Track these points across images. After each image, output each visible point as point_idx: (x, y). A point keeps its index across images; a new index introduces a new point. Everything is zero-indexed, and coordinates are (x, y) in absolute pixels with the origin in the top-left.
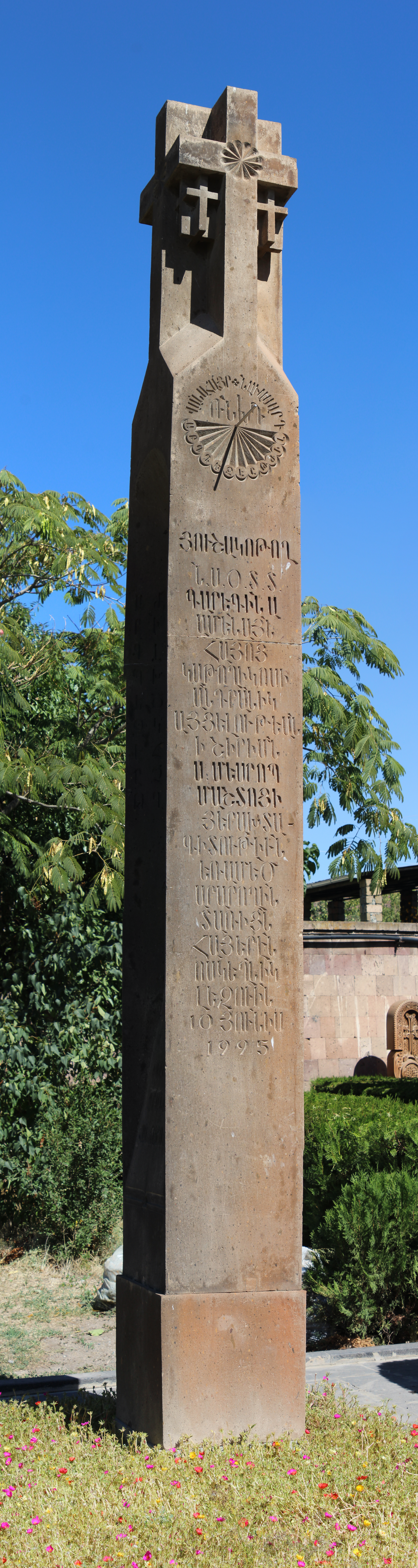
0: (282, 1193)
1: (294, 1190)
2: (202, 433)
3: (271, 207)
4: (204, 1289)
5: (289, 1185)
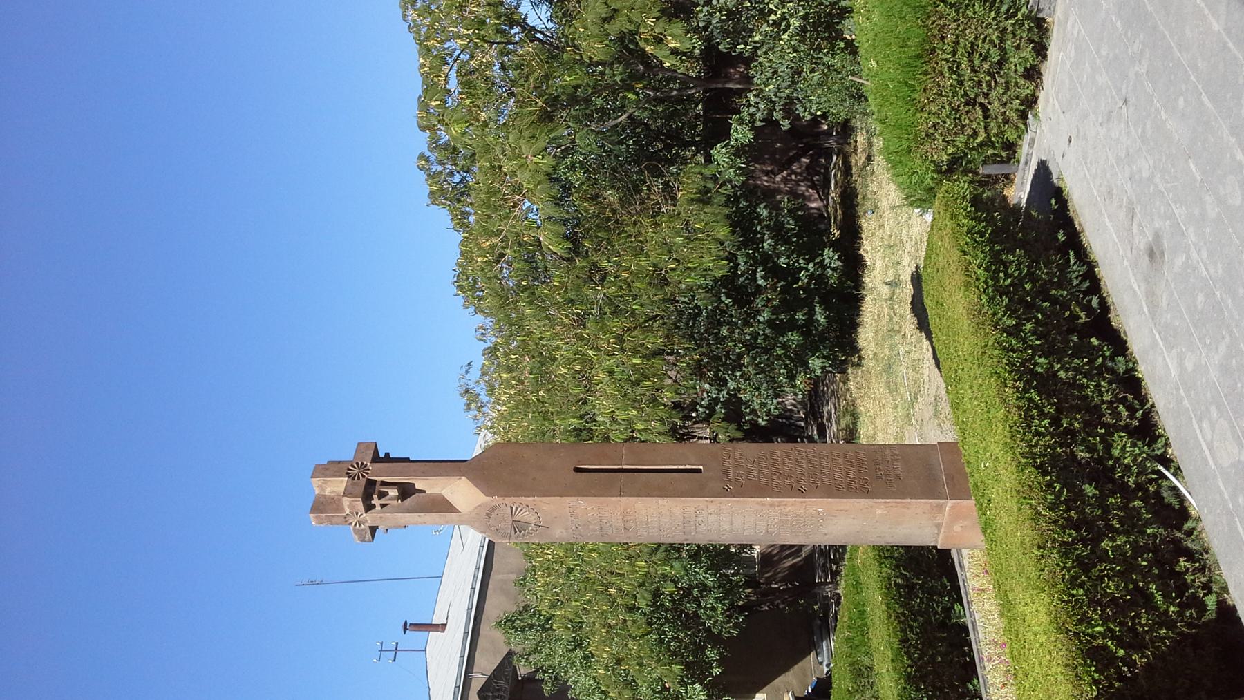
0: (896, 507)
1: (896, 502)
2: (520, 532)
3: (376, 501)
4: (938, 534)
5: (894, 504)
